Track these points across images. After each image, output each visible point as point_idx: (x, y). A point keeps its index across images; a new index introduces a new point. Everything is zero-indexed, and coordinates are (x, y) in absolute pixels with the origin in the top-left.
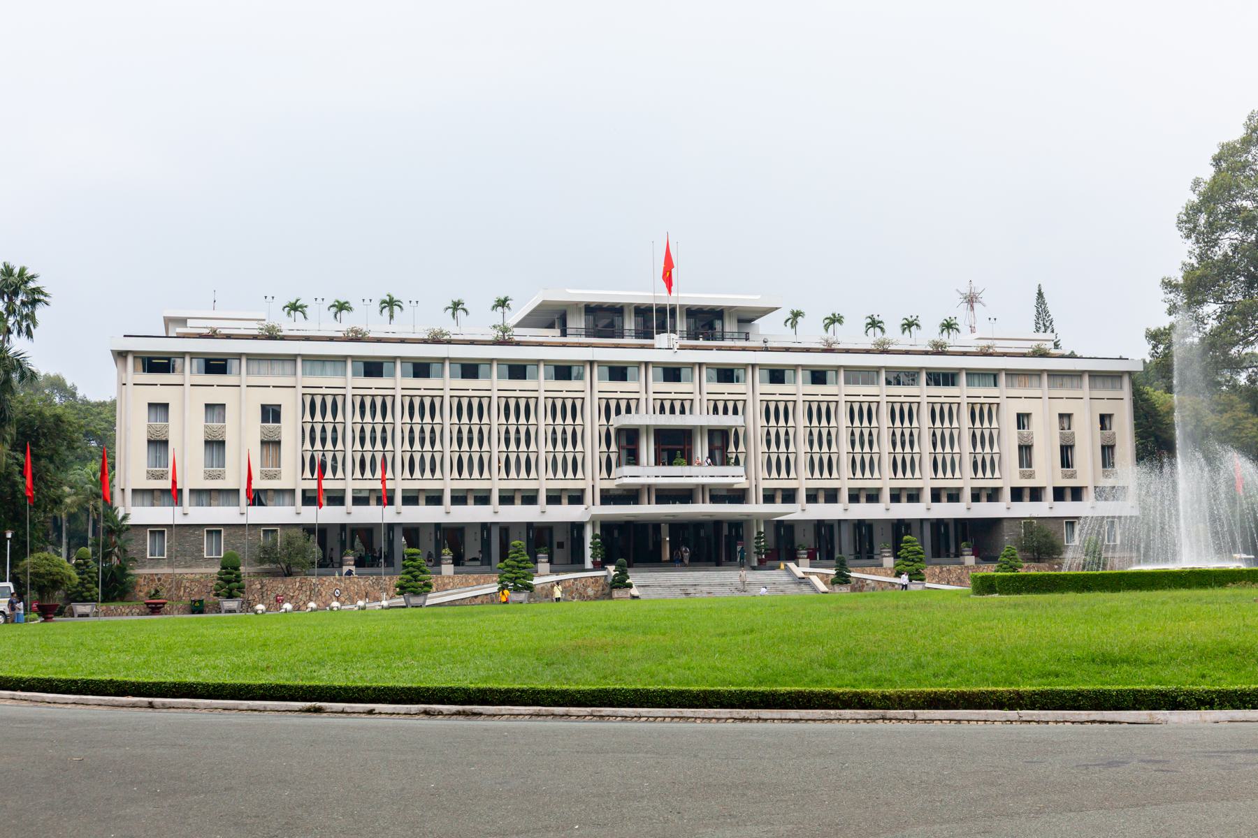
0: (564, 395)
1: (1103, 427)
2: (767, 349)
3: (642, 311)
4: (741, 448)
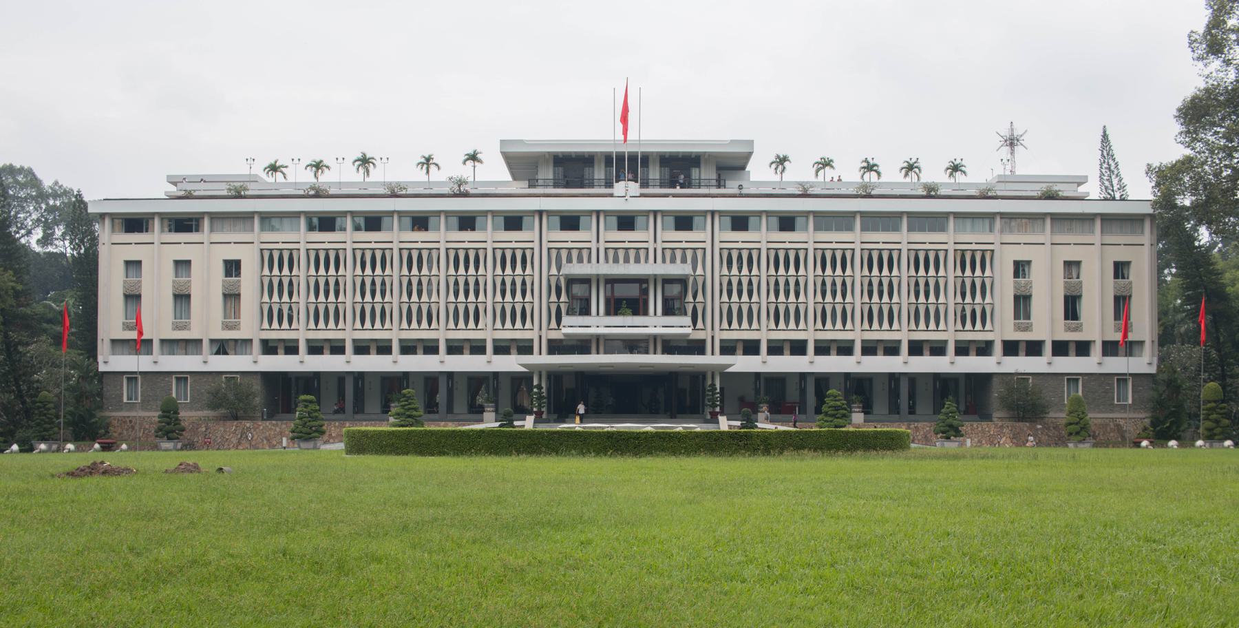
0: (834, 246)
1: (1016, 275)
2: (741, 196)
3: (608, 159)
4: (700, 298)
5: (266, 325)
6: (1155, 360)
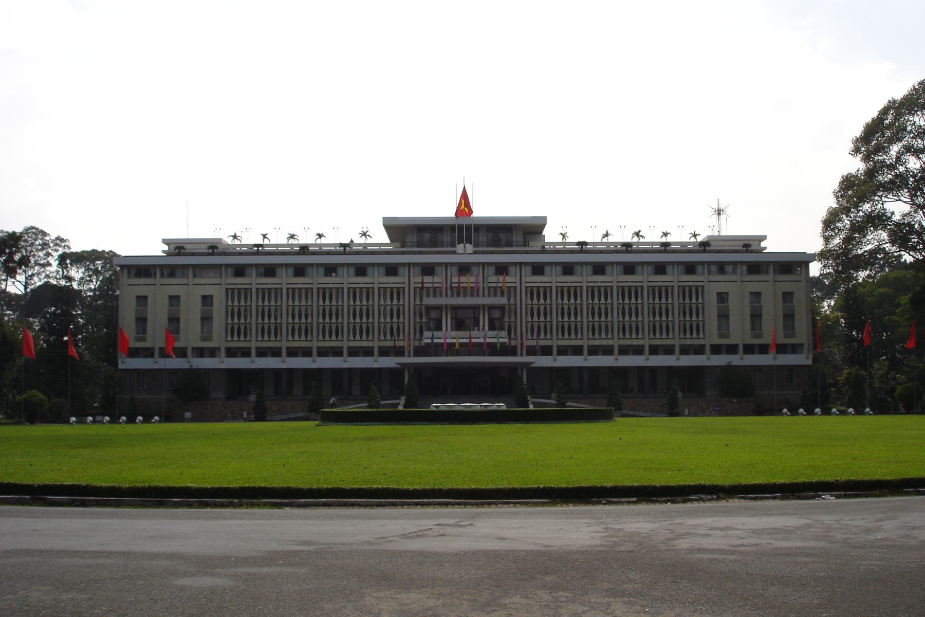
5: (229, 338)
6: (811, 356)
